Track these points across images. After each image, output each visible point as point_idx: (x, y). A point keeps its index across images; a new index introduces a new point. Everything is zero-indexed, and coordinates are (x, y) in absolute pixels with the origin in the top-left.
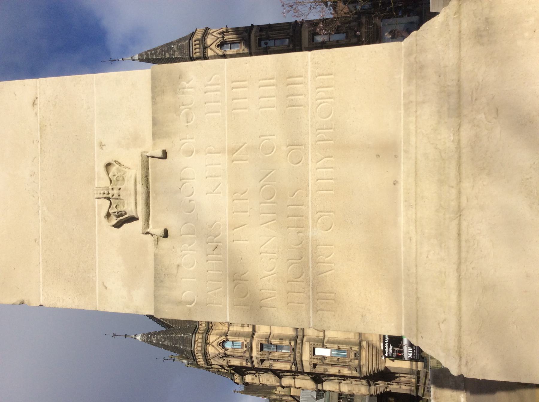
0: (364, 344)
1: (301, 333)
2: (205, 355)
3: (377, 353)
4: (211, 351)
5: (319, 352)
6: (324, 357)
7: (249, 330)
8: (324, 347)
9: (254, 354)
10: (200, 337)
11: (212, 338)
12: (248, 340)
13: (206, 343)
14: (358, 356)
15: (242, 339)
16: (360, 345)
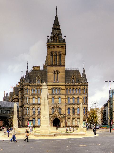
0: (29, 117)
1: (30, 105)
2: (25, 85)
3: (28, 119)
4: (26, 87)
5: (27, 108)
6: (26, 110)
7: (30, 94)
8: (28, 109)
9: (26, 96)
10: (29, 84)
11: (28, 87)
12: (28, 94)
13: (27, 85)
14: (27, 116)
15: (28, 93)
16: (29, 116)
